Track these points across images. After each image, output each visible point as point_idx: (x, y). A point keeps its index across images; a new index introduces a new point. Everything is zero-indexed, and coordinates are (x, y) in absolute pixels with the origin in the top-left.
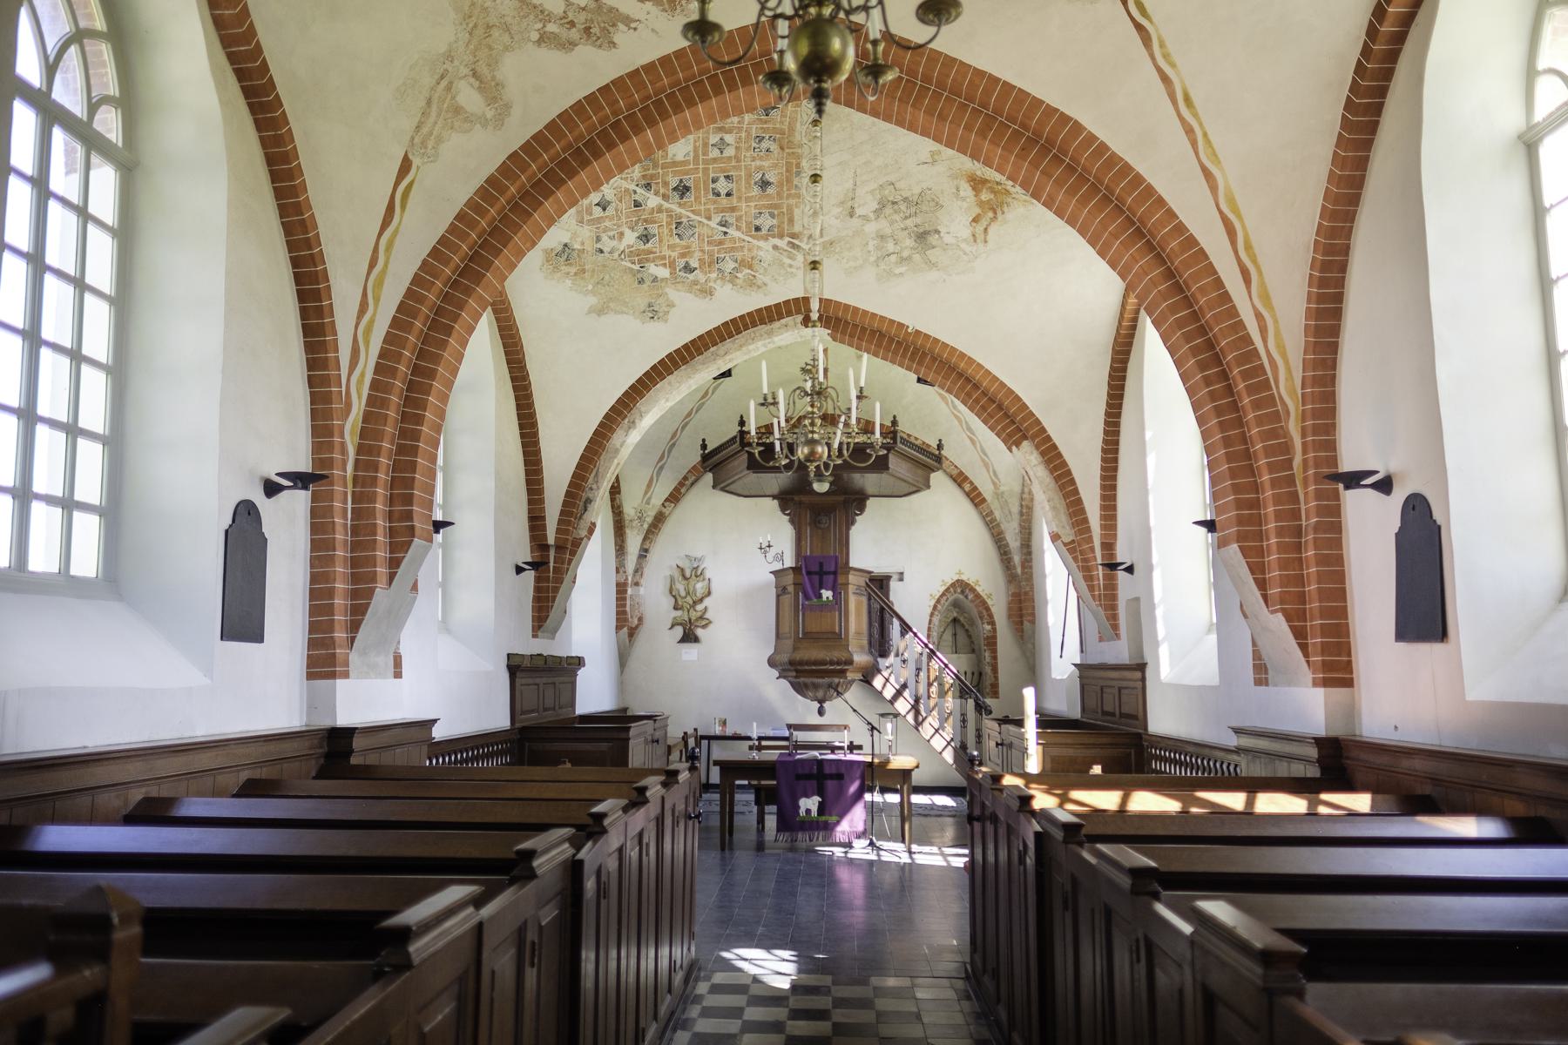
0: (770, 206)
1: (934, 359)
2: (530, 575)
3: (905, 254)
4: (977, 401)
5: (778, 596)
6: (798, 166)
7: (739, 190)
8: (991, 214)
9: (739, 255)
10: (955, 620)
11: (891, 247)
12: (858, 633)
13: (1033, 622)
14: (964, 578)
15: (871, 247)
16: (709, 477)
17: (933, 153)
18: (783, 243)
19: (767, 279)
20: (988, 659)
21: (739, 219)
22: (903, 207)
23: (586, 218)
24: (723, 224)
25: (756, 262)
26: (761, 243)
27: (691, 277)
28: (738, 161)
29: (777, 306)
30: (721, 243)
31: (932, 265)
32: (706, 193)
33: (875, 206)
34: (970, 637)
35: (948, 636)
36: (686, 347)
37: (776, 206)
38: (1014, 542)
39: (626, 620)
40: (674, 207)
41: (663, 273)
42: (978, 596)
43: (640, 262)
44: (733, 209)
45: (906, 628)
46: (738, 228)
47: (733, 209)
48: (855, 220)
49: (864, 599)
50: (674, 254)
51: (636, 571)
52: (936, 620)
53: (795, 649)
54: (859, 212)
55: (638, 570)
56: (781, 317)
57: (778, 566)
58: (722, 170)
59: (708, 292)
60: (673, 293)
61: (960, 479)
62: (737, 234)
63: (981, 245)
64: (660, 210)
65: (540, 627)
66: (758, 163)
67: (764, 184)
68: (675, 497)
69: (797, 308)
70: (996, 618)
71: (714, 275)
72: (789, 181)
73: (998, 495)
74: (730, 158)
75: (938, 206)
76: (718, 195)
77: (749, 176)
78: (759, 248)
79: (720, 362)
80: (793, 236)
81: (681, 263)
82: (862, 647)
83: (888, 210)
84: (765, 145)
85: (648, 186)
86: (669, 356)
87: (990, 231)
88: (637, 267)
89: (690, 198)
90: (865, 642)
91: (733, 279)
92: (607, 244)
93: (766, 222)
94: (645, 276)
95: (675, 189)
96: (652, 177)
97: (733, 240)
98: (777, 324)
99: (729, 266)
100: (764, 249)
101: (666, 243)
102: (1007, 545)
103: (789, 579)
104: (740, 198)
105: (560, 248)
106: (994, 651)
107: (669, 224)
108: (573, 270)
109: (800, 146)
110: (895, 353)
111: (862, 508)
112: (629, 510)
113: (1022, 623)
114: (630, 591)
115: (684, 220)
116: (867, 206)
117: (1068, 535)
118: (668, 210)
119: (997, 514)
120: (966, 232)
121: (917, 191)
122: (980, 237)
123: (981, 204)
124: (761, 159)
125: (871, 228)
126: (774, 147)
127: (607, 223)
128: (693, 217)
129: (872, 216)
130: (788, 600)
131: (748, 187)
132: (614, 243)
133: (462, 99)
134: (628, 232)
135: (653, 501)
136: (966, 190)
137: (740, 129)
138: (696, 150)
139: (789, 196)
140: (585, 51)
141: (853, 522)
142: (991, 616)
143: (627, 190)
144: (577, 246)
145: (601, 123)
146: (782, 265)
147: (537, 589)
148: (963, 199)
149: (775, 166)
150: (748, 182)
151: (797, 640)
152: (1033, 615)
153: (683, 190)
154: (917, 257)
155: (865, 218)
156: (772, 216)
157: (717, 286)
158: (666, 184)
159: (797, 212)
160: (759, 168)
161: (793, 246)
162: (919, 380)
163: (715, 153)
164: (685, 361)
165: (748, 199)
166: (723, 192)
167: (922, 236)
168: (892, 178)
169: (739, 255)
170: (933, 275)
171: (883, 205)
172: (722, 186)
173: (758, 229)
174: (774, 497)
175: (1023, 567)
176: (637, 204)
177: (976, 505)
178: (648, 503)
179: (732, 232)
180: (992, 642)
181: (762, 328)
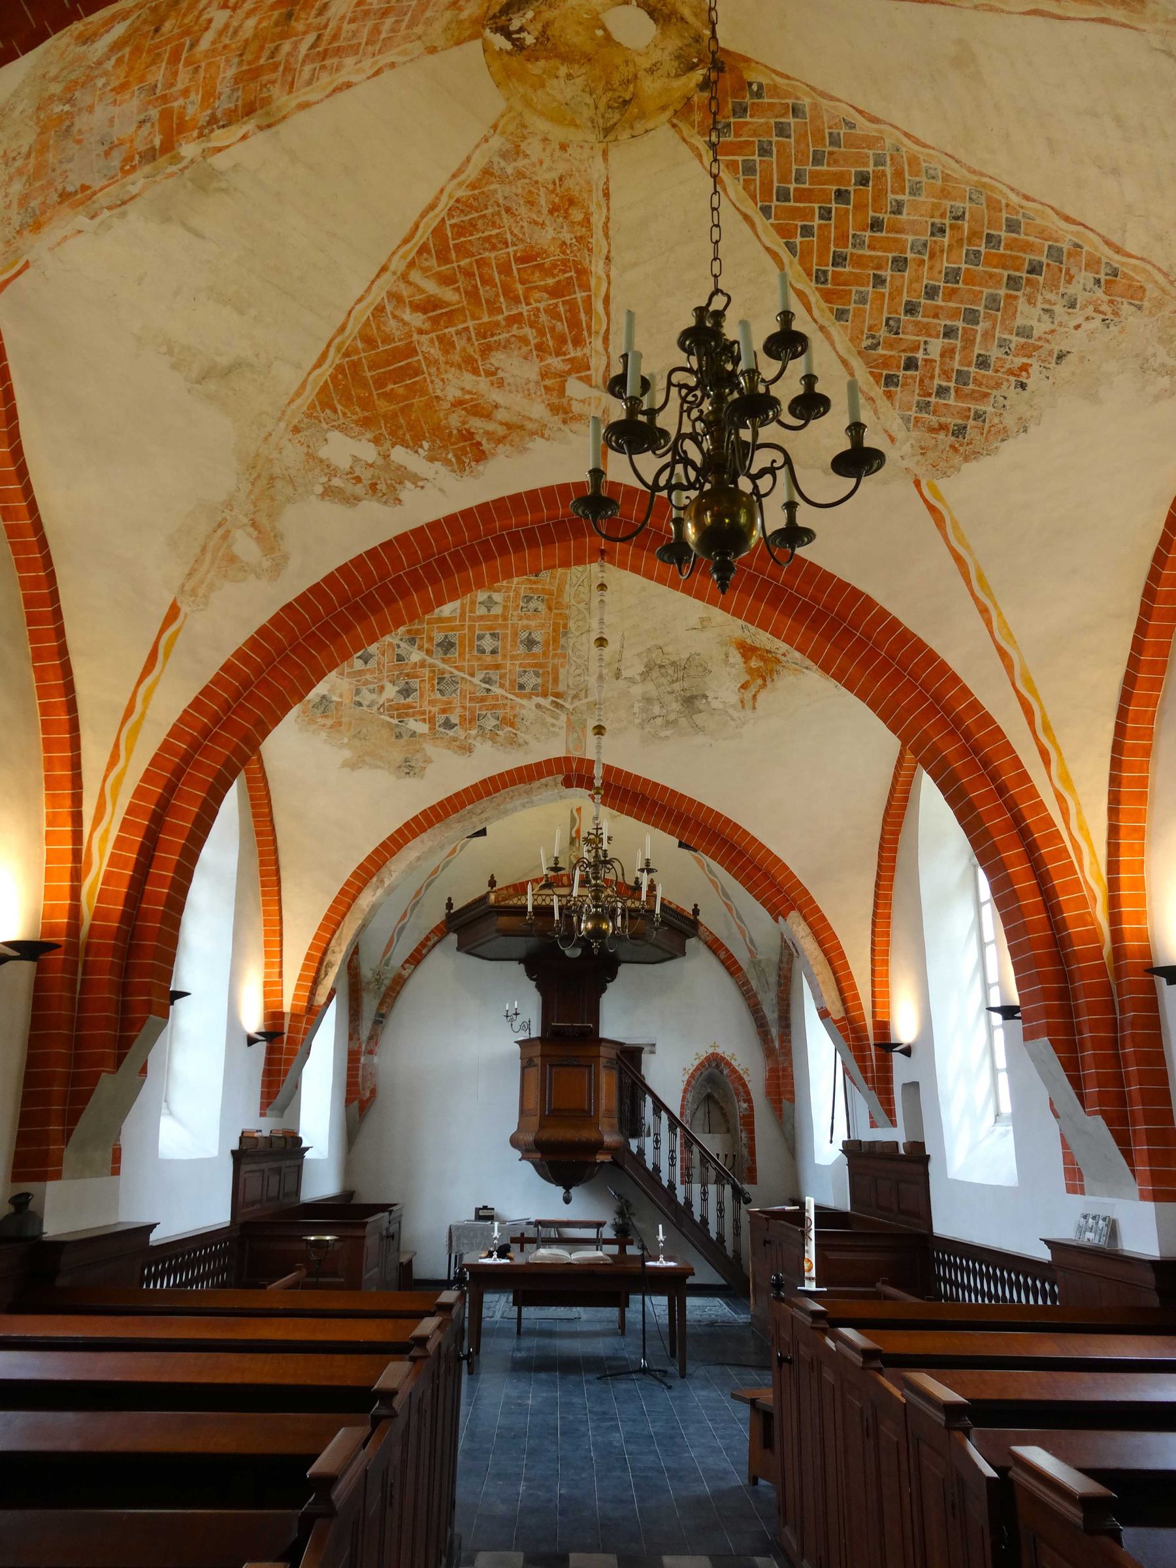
1: (698, 824)
2: (262, 1047)
3: (672, 717)
4: (742, 869)
5: (523, 1069)
6: (565, 626)
7: (504, 648)
8: (760, 681)
9: (500, 713)
10: (709, 1097)
11: (656, 710)
12: (608, 1110)
13: (792, 1101)
14: (720, 1051)
15: (636, 710)
16: (453, 938)
17: (702, 620)
18: (546, 702)
19: (527, 737)
20: (745, 1140)
21: (502, 676)
22: (670, 671)
24: (486, 680)
25: (517, 720)
26: (524, 702)
27: (451, 733)
28: (505, 619)
29: (538, 765)
30: (483, 700)
31: (698, 729)
32: (471, 651)
33: (642, 669)
34: (724, 1115)
35: (700, 1114)
36: (441, 804)
37: (540, 665)
38: (771, 1015)
39: (358, 1092)
41: (422, 728)
42: (734, 1071)
43: (399, 716)
44: (497, 667)
45: (659, 1106)
46: (502, 686)
47: (497, 667)
48: (621, 682)
49: (615, 1073)
50: (435, 710)
51: (371, 1038)
52: (689, 1096)
53: (542, 1126)
54: (625, 674)
55: (373, 1038)
56: (541, 776)
57: (523, 1036)
58: (489, 628)
59: (467, 749)
60: (430, 749)
61: (715, 946)
63: (749, 712)
64: (423, 664)
65: (268, 1104)
66: (525, 622)
67: (530, 643)
68: (416, 958)
69: (574, 773)
71: (473, 732)
72: (556, 640)
73: (755, 963)
76: (483, 652)
77: (515, 634)
78: (522, 706)
79: (475, 819)
81: (441, 718)
82: (612, 1126)
83: (655, 674)
84: (532, 605)
85: (412, 641)
86: (424, 813)
87: (760, 697)
88: (395, 721)
89: (455, 654)
90: (616, 1121)
91: (493, 736)
92: (367, 697)
93: (531, 680)
94: (403, 731)
95: (439, 645)
97: (496, 697)
98: (536, 784)
99: (490, 723)
100: (528, 707)
101: (426, 699)
102: (764, 1017)
103: (537, 1050)
104: (505, 656)
106: (751, 1132)
107: (431, 679)
108: (329, 722)
109: (568, 607)
110: (667, 820)
111: (613, 975)
112: (367, 972)
114: (362, 1060)
115: (447, 676)
116: (634, 669)
117: (837, 1011)
118: (431, 666)
119: (754, 983)
121: (685, 656)
122: (749, 704)
123: (750, 671)
124: (528, 618)
125: (637, 690)
126: (542, 607)
127: (368, 677)
128: (456, 672)
129: (638, 677)
130: (534, 1073)
131: (514, 645)
132: (374, 696)
133: (237, 549)
135: (392, 962)
139: (555, 656)
140: (371, 508)
141: (604, 989)
142: (748, 1093)
143: (390, 644)
144: (335, 698)
145: (381, 579)
146: (544, 724)
147: (269, 1062)
148: (733, 666)
149: (542, 626)
150: (514, 640)
151: (543, 1117)
152: (792, 1093)
153: (447, 646)
154: (683, 721)
155: (631, 680)
156: (537, 674)
158: (430, 639)
159: (562, 672)
160: (528, 627)
161: (556, 705)
162: (681, 845)
164: (439, 819)
165: (513, 658)
166: (488, 649)
167: (690, 701)
168: (660, 642)
169: (500, 713)
170: (700, 739)
171: (649, 668)
172: (488, 643)
173: (522, 687)
174: (521, 961)
175: (782, 1041)
176: (400, 658)
177: (732, 974)
178: (387, 964)
179: (496, 690)
180: (748, 1121)
181: (521, 787)
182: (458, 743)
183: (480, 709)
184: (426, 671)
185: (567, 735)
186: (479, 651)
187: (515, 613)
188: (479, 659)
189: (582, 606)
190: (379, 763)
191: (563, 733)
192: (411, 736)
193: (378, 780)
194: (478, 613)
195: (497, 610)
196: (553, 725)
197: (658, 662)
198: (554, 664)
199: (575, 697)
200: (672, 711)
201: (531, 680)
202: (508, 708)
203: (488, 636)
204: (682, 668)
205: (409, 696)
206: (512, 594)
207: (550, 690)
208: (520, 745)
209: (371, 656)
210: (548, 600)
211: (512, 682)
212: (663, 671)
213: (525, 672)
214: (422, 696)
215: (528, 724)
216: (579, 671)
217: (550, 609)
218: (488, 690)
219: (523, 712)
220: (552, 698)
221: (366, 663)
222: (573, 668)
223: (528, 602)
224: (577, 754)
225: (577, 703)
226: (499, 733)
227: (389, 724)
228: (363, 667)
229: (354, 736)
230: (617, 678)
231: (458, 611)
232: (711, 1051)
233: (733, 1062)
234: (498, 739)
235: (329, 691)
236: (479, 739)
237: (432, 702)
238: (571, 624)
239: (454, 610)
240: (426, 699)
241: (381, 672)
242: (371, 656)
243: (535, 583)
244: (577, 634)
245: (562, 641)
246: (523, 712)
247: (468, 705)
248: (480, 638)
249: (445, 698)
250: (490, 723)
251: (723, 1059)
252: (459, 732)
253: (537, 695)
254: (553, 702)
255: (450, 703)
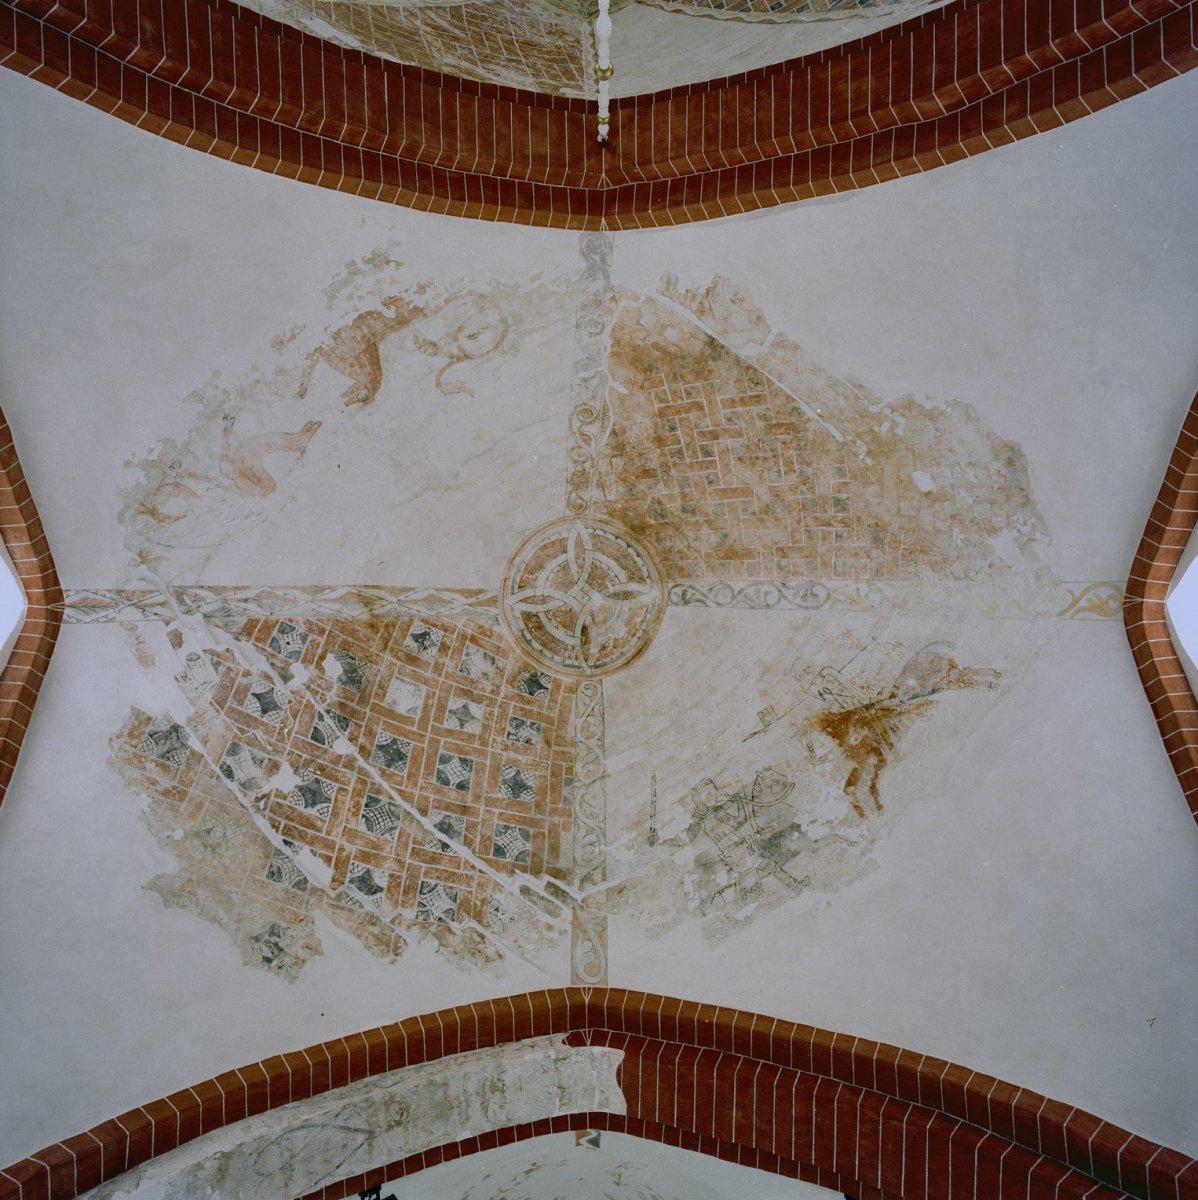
0: (523, 821)
3: (749, 882)
6: (570, 770)
7: (478, 784)
9: (461, 889)
18: (538, 884)
21: (471, 827)
22: (732, 810)
23: (230, 703)
24: (445, 828)
26: (501, 877)
28: (484, 743)
30: (434, 859)
31: (798, 884)
33: (689, 821)
37: (532, 823)
40: (373, 772)
41: (320, 873)
43: (287, 831)
44: (464, 810)
46: (468, 843)
47: (464, 810)
48: (657, 848)
50: (351, 849)
54: (663, 835)
59: (390, 946)
60: (327, 927)
62: (464, 852)
64: (350, 763)
66: (512, 755)
67: (517, 786)
71: (409, 914)
72: (555, 789)
74: (471, 737)
75: (787, 786)
76: (446, 782)
77: (497, 768)
78: (497, 886)
80: (557, 873)
81: (358, 869)
83: (709, 823)
84: (524, 733)
85: (343, 722)
88: (276, 839)
89: (403, 771)
92: (245, 769)
95: (381, 747)
96: (354, 713)
97: (456, 861)
100: (508, 888)
104: (477, 797)
105: (165, 727)
107: (358, 793)
116: (675, 821)
118: (361, 771)
120: (844, 808)
121: (749, 780)
124: (516, 750)
126: (537, 738)
127: (259, 734)
128: (399, 800)
129: (684, 836)
132: (258, 772)
134: (286, 768)
136: (825, 744)
137: (492, 702)
138: (426, 708)
139: (553, 812)
143: (309, 706)
144: (194, 743)
146: (534, 923)
149: (536, 765)
150: (493, 777)
154: (771, 882)
155: (674, 843)
156: (526, 836)
157: (412, 936)
158: (370, 733)
159: (565, 838)
160: (512, 763)
163: (451, 723)
165: (490, 802)
166: (454, 780)
167: (773, 845)
168: (708, 773)
169: (461, 889)
170: (807, 899)
171: (699, 817)
172: (454, 771)
176: (317, 736)
179: (458, 848)
182: (376, 930)
183: (426, 874)
184: (353, 777)
185: (574, 944)
186: (439, 778)
187: (499, 739)
188: (438, 791)
189: (593, 743)
190: (221, 913)
191: (567, 940)
192: (297, 885)
193: (209, 947)
194: (446, 725)
195: (473, 728)
196: (550, 927)
197: (712, 803)
198: (552, 825)
199: (586, 879)
200: (748, 871)
201: (516, 845)
202: (474, 885)
203: (456, 761)
204: (747, 800)
205: (314, 804)
206: (496, 711)
207: (543, 861)
208: (488, 960)
209: (276, 707)
210: (545, 730)
211: (486, 839)
212: (721, 813)
213: (507, 828)
214: (335, 814)
215: (505, 918)
216: (592, 838)
217: (548, 743)
218: (445, 846)
219: (499, 896)
220: (547, 878)
221: (264, 711)
222: (583, 832)
223: (517, 727)
224: (591, 981)
225: (591, 890)
226: (454, 926)
227: (266, 843)
228: (257, 715)
229: (197, 834)
230: (652, 844)
231: (419, 712)
234: (450, 938)
235: (190, 720)
236: (416, 930)
237: (349, 833)
238: (578, 768)
239: (413, 710)
240: (341, 823)
241: (282, 740)
242: (276, 707)
243: (529, 702)
244: (588, 781)
245: (565, 791)
246: (499, 896)
247: (408, 861)
248: (444, 760)
249: (372, 836)
250: (440, 904)
252: (383, 907)
253: (524, 870)
254: (550, 885)
255: (376, 847)
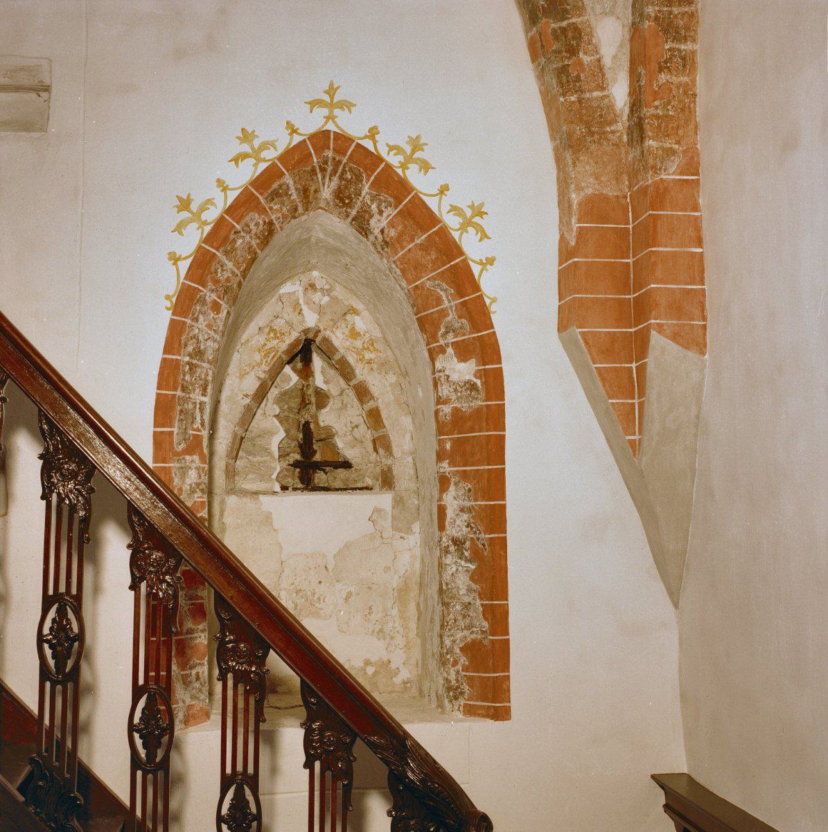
14: (353, 125)
42: (418, 215)
70: (503, 324)
106: (493, 486)
113: (640, 346)
142: (477, 313)
180: (474, 442)
232: (311, 123)
233: (414, 176)
251: (368, 159)
